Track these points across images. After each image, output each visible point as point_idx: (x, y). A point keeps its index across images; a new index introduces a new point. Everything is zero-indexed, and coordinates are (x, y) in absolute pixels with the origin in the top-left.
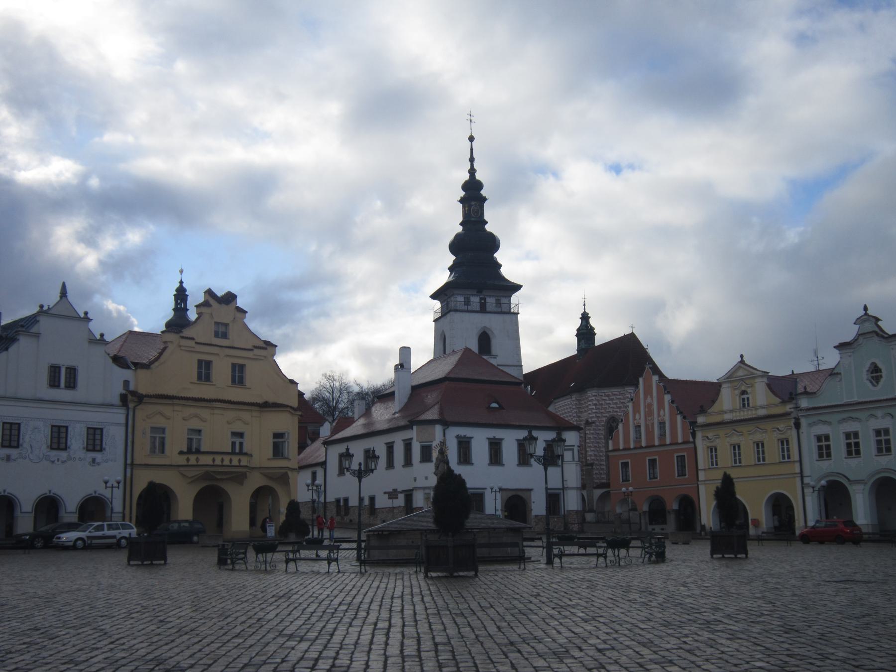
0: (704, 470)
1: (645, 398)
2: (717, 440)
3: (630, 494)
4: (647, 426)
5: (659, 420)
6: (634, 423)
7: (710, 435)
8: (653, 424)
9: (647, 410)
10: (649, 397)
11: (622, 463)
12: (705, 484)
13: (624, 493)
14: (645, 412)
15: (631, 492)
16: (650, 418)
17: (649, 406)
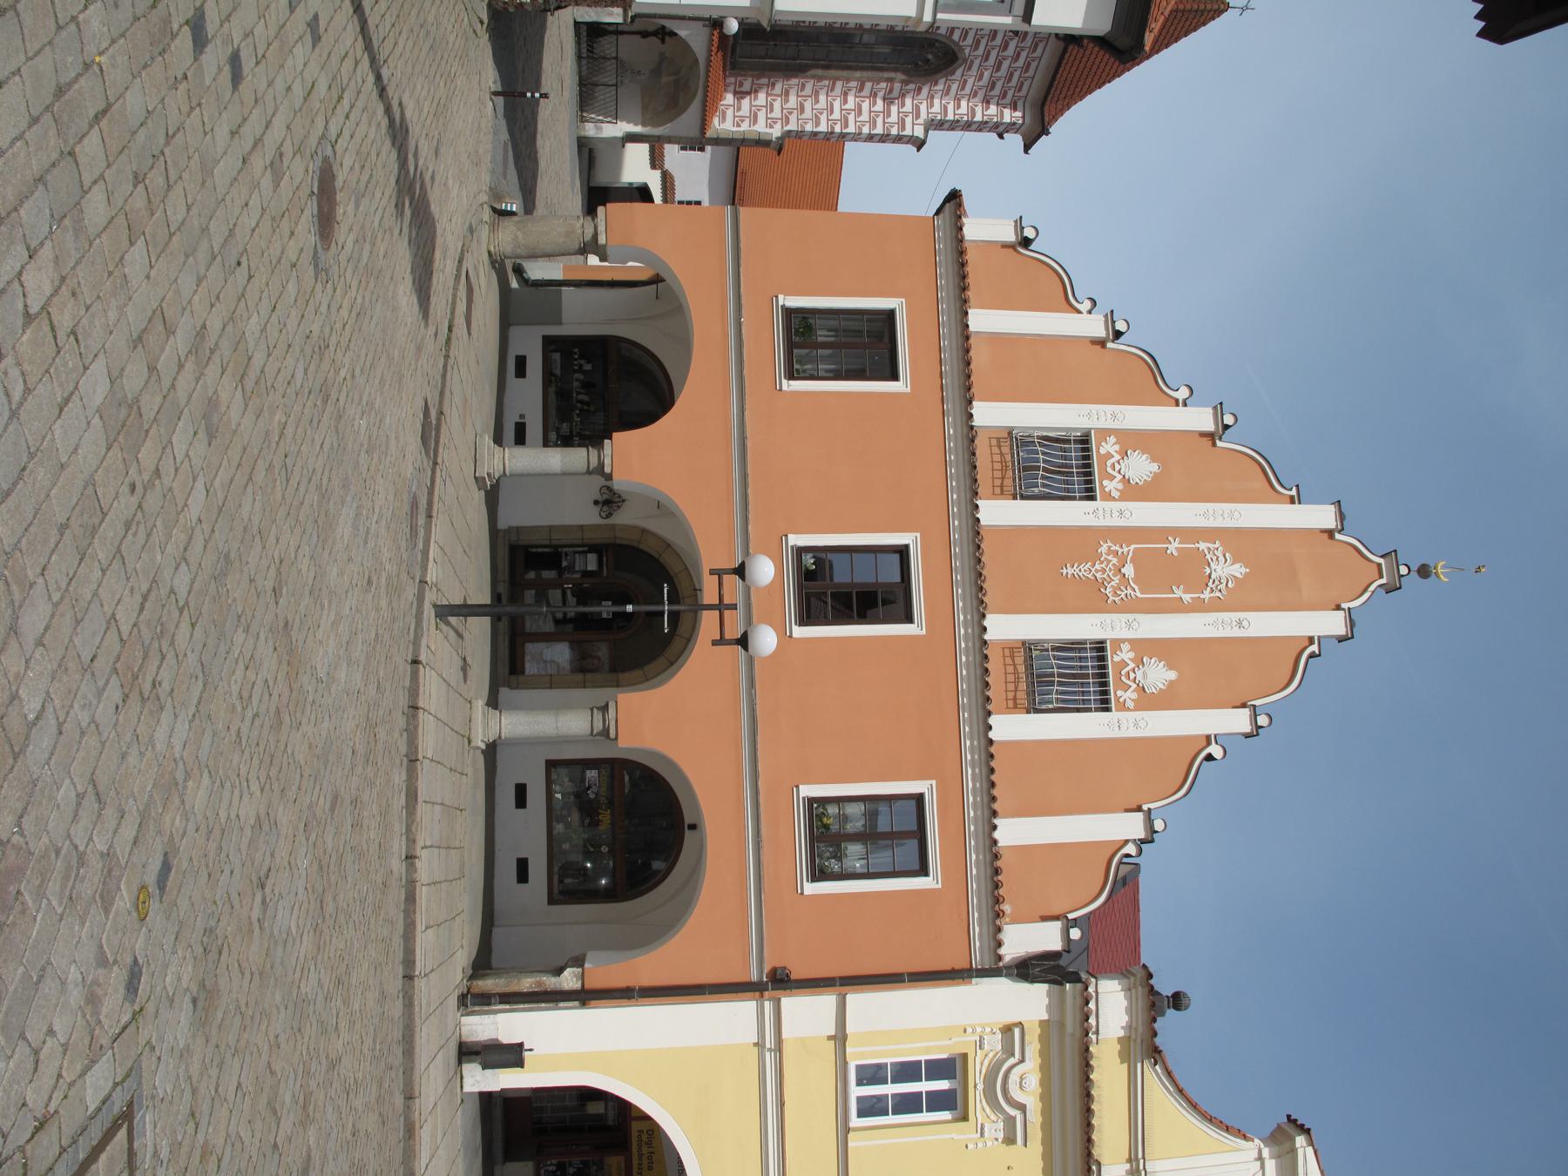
0: (840, 1038)
1: (1238, 541)
2: (996, 1129)
3: (734, 631)
4: (1084, 541)
5: (1117, 643)
6: (1105, 433)
7: (1027, 1081)
8: (1093, 599)
9: (1174, 547)
10: (1238, 570)
11: (890, 315)
12: (760, 1045)
13: (740, 571)
14: (1164, 533)
15: (743, 641)
16: (1129, 570)
17: (1191, 570)
